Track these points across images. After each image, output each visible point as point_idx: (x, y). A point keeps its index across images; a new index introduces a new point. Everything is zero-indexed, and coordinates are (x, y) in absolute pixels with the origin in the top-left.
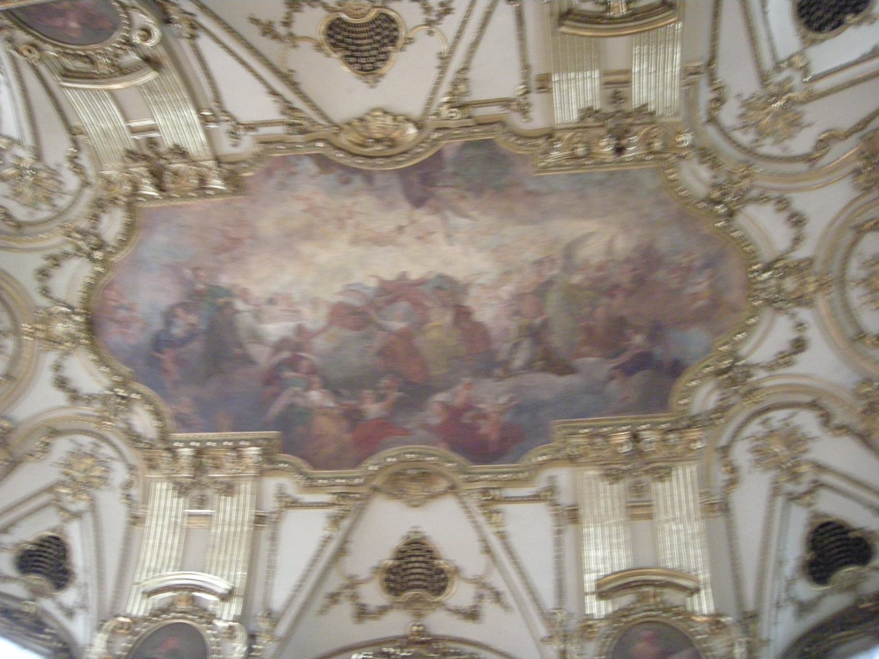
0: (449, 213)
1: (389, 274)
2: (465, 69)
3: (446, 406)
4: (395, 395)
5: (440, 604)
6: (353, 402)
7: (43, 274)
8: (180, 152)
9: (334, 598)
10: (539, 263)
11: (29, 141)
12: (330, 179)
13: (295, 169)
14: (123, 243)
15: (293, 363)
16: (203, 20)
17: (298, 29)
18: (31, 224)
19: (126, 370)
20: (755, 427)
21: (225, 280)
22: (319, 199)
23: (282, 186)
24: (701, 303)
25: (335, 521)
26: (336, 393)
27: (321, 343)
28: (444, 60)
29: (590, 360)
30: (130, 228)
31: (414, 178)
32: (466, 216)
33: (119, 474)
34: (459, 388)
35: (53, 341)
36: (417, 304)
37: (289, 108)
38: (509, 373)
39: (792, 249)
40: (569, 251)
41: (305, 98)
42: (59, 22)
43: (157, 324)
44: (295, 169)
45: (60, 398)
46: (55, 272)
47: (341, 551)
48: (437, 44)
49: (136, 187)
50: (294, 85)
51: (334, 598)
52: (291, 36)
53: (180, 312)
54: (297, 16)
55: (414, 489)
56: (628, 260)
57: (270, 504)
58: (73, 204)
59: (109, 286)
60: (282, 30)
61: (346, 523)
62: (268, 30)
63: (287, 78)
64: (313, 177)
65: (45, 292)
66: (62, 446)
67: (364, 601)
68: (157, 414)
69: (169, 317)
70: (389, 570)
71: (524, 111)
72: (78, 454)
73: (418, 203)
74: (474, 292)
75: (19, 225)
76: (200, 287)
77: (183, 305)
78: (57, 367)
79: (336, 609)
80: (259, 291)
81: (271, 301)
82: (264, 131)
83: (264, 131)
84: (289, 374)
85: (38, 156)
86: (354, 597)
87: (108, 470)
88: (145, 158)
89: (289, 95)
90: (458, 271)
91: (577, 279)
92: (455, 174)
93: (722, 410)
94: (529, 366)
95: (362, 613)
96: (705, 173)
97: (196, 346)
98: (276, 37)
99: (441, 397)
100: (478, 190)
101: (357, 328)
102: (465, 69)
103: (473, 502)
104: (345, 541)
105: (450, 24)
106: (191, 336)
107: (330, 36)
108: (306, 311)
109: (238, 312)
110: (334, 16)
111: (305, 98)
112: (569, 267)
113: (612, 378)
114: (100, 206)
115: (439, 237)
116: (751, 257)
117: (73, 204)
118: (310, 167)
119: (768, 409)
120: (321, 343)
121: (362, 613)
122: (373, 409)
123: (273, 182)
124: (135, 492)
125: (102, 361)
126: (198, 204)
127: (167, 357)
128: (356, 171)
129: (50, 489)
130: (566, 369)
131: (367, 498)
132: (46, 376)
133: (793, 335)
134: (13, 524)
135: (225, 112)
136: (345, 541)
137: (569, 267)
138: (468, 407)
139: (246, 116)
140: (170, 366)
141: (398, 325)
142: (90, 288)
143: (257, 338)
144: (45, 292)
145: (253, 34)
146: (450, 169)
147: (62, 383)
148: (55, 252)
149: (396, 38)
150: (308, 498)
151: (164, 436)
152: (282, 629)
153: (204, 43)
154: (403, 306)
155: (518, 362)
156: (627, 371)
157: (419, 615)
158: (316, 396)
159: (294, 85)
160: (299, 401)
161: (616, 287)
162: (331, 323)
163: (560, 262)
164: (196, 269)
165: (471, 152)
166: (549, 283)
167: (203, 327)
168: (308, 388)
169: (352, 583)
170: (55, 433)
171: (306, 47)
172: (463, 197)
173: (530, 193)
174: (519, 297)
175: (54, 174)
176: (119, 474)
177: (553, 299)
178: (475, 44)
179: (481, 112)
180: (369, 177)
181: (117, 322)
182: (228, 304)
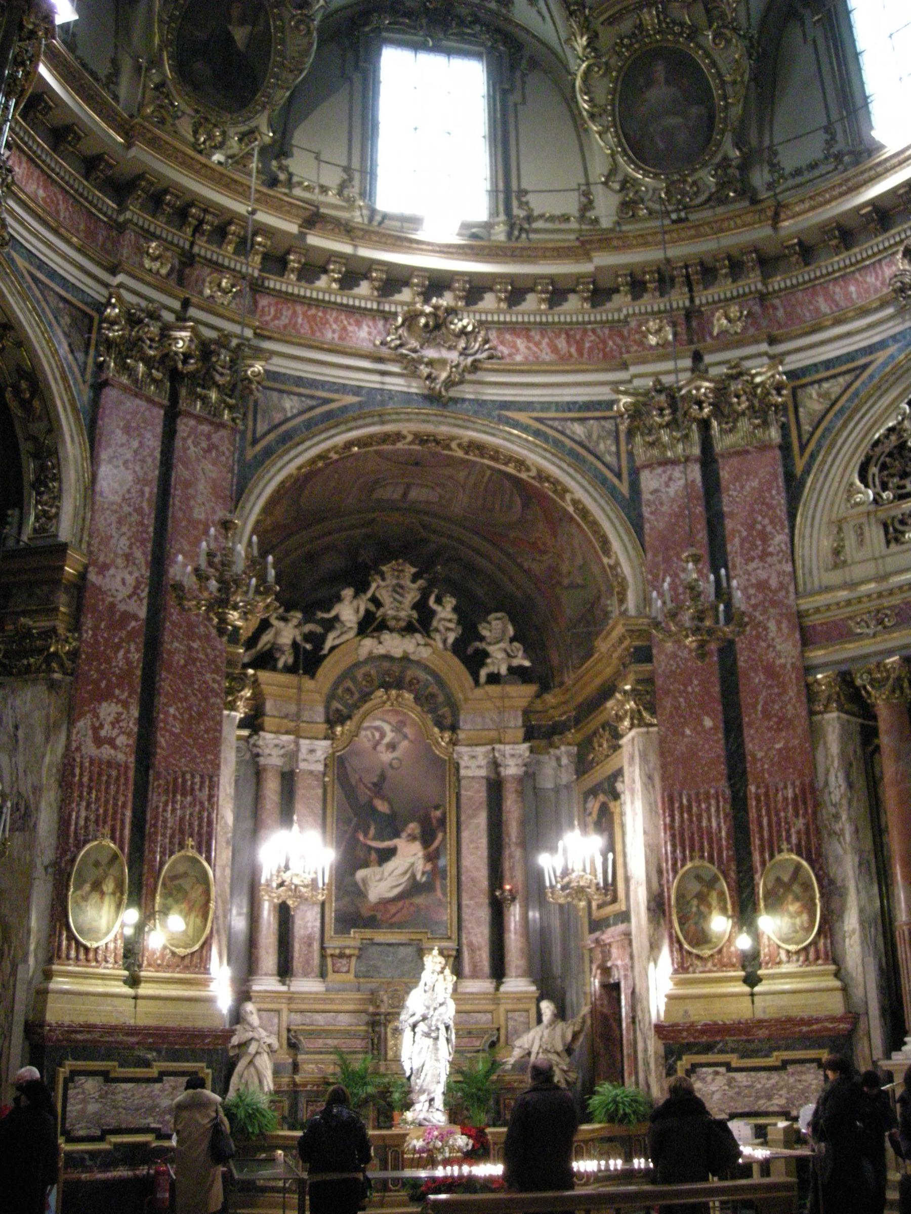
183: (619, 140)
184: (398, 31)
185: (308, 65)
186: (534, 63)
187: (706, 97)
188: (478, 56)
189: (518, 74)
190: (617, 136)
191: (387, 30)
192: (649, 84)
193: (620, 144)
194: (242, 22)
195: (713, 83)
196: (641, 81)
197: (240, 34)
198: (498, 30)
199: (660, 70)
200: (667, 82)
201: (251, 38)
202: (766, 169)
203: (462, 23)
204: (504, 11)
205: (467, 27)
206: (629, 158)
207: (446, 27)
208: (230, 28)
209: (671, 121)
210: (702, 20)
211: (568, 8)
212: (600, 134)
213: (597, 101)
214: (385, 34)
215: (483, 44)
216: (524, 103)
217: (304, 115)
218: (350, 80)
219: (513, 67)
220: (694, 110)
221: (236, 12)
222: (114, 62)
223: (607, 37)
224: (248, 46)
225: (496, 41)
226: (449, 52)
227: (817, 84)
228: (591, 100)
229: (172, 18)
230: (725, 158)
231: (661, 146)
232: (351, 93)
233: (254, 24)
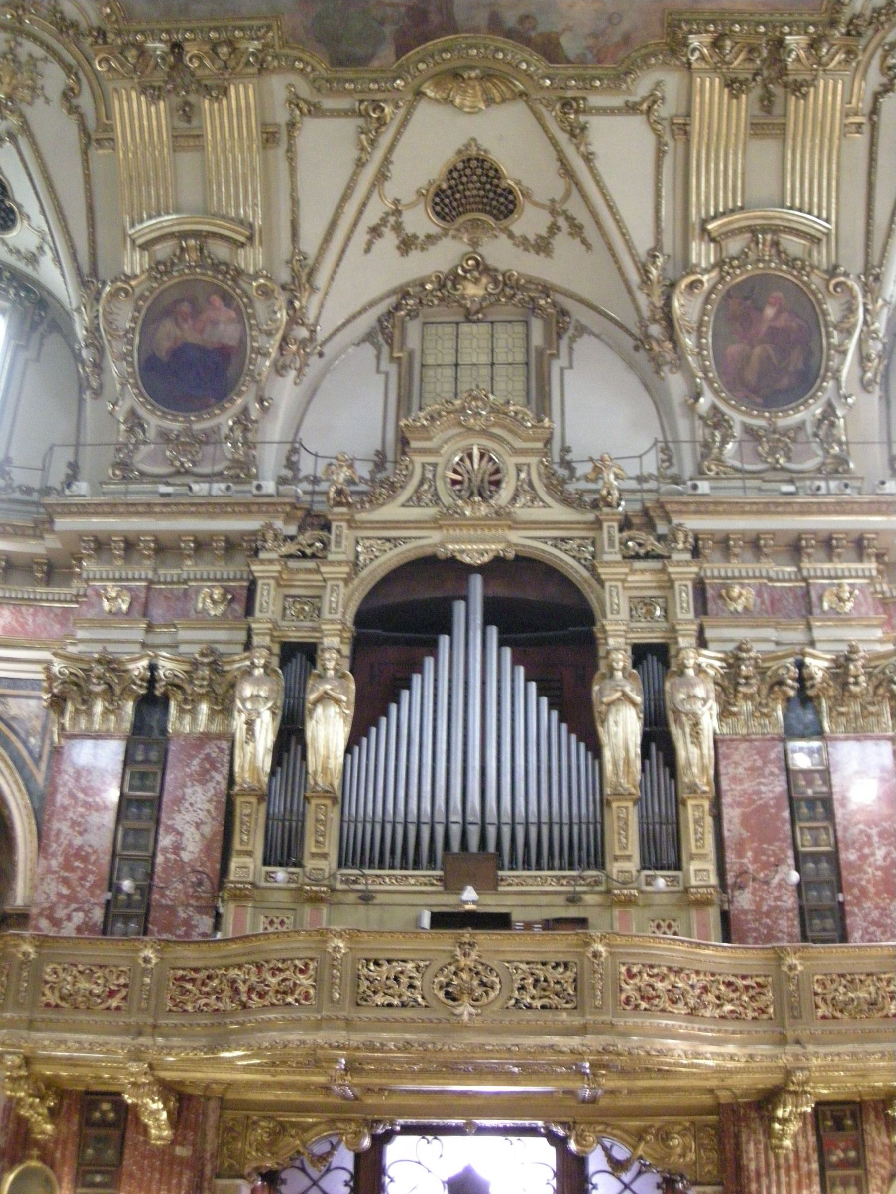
2: (360, 164)
8: (734, 85)
12: (544, 25)
13: (591, 41)
17: (546, 219)
23: (612, 19)
28: (382, 176)
31: (435, 19)
37: (577, 133)
41: (554, 143)
42: (781, 323)
44: (591, 41)
48: (392, 189)
50: (562, 160)
52: (553, 212)
54: (544, 232)
60: (561, 222)
62: (576, 229)
63: (567, 171)
64: (569, 29)
71: (294, 101)
82: (617, 101)
83: (617, 101)
92: (382, 23)
98: (570, 219)
102: (360, 164)
105: (372, 217)
110: (504, 223)
111: (554, 143)
118: (570, 45)
123: (625, 26)
128: (509, 34)
139: (636, 124)
146: (388, 30)
149: (437, 195)
153: (643, 242)
159: (562, 160)
165: (360, 51)
171: (541, 196)
178: (345, 198)
179: (344, 103)
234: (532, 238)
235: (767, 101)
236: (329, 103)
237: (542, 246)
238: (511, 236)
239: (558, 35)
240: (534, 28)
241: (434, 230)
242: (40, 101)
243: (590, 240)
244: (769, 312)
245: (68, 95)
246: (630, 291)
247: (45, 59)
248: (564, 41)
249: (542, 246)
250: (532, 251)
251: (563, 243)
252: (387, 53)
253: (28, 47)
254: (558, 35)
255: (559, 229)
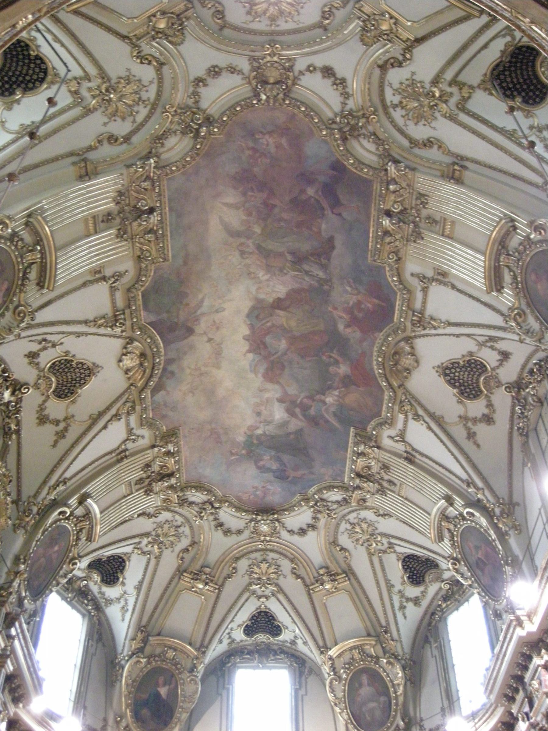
0: (199, 312)
1: (245, 346)
2: (86, 322)
3: (347, 326)
4: (335, 355)
5: (493, 369)
6: (337, 379)
7: (227, 532)
9: (471, 435)
10: (242, 253)
11: (137, 540)
12: (170, 384)
13: (162, 403)
14: (209, 491)
15: (305, 409)
16: (53, 481)
18: (193, 537)
19: (298, 497)
20: (397, 115)
21: (241, 439)
22: (184, 387)
24: (284, 141)
25: (417, 417)
26: (330, 388)
27: (292, 390)
29: (324, 226)
30: (199, 487)
32: (202, 301)
33: (369, 515)
34: (336, 313)
35: (274, 533)
36: (268, 331)
37: (117, 416)
38: (328, 281)
39: (240, 72)
40: (234, 234)
41: (108, 408)
42: (55, 556)
43: (270, 476)
44: (162, 403)
45: (311, 534)
46: (226, 526)
47: (439, 421)
49: (171, 487)
50: (101, 414)
51: (471, 435)
52: (66, 419)
53: (261, 463)
55: (407, 361)
56: (244, 194)
57: (400, 447)
58: (180, 514)
59: (239, 499)
60: (62, 425)
61: (421, 412)
62: (61, 435)
63: (95, 420)
64: (168, 392)
65: (239, 532)
66: (344, 540)
67: (479, 416)
68: (330, 488)
69: (263, 469)
70: (462, 393)
72: (351, 533)
73: (190, 331)
74: (262, 296)
75: (193, 543)
76: (244, 452)
77: (256, 463)
78: (291, 532)
79: (479, 438)
80: (250, 421)
81: (259, 414)
84: (312, 412)
85: (147, 534)
86: (475, 421)
87: (364, 520)
88: (150, 484)
89: (107, 417)
90: (246, 305)
91: (257, 229)
92: (168, 312)
93: (378, 140)
94: (324, 267)
95: (488, 419)
96: (172, 141)
97: (286, 458)
98: (66, 429)
99: (341, 327)
100: (181, 296)
101: (283, 367)
103: (420, 331)
104: (432, 416)
106: (279, 459)
107: (66, 396)
108: (267, 395)
109: (264, 432)
111: (108, 408)
112: (247, 234)
113: (340, 215)
114: (183, 502)
115: (217, 317)
116: (246, 104)
117: (180, 514)
118: (160, 396)
119: (383, 101)
120: (292, 390)
121: (488, 419)
122: (343, 369)
123: (171, 414)
124: (381, 512)
125: (290, 509)
126: (185, 453)
127: (292, 474)
129: (370, 555)
130: (330, 243)
131: (407, 392)
132: (296, 539)
133: (319, 75)
134: (387, 581)
135: (118, 448)
136: (432, 416)
137: (247, 234)
138: (350, 311)
140: (299, 473)
141: (283, 344)
142: (239, 509)
143: (284, 425)
144: (239, 532)
145: (64, 444)
146: (165, 316)
147: (302, 532)
148: (213, 523)
150: (400, 425)
151: (344, 488)
152: (480, 484)
154: (268, 339)
155: (321, 274)
156: (336, 203)
157: (499, 384)
158: (329, 400)
159: (101, 414)
160: (332, 409)
161: (265, 203)
162: (278, 383)
163: (243, 240)
164: (232, 454)
166: (259, 247)
167: (273, 453)
168: (324, 403)
169: (464, 418)
170: (335, 543)
172: (187, 304)
173: (185, 263)
174: (269, 268)
175: (160, 525)
176: (369, 515)
177: (270, 245)
179: (120, 304)
180: (169, 362)
181: (264, 497)
182: (258, 437)
183: (349, 716)
184: (245, 662)
185: (197, 699)
186: (311, 671)
187: (386, 693)
188: (285, 668)
189: (303, 678)
190: (348, 714)
191: (239, 663)
192: (361, 685)
193: (350, 719)
194: (164, 685)
195: (389, 685)
196: (357, 685)
197: (163, 691)
198: (293, 655)
199: (364, 679)
200: (369, 685)
201: (168, 695)
202: (418, 728)
203: (276, 653)
204: (294, 647)
205: (278, 655)
206: (354, 726)
207: (267, 657)
208: (159, 689)
209: (372, 705)
210: (381, 653)
211: (320, 650)
212: (340, 713)
213: (337, 696)
214: (238, 665)
215: (286, 663)
216: (306, 694)
217: (197, 721)
218: (221, 695)
219: (301, 674)
220: (383, 699)
221: (161, 680)
222: (105, 720)
223: (339, 664)
224: (168, 695)
225: (291, 662)
226: (270, 668)
227: (437, 683)
228: (335, 696)
229: (130, 693)
230: (398, 726)
231: (369, 718)
232: (221, 703)
233: (170, 684)
234: (46, 412)
235: (140, 481)
236: (119, 295)
237: (43, 420)
238: (45, 401)
239: (165, 389)
240: (168, 378)
241: (42, 365)
242: (106, 120)
243: (59, 445)
244: (56, 548)
245: (112, 139)
246: (45, 482)
247: (134, 121)
248: (162, 393)
249: (43, 420)
250: (37, 416)
251: (49, 430)
252: (152, 318)
253: (143, 112)
254: (165, 389)
255: (57, 425)
